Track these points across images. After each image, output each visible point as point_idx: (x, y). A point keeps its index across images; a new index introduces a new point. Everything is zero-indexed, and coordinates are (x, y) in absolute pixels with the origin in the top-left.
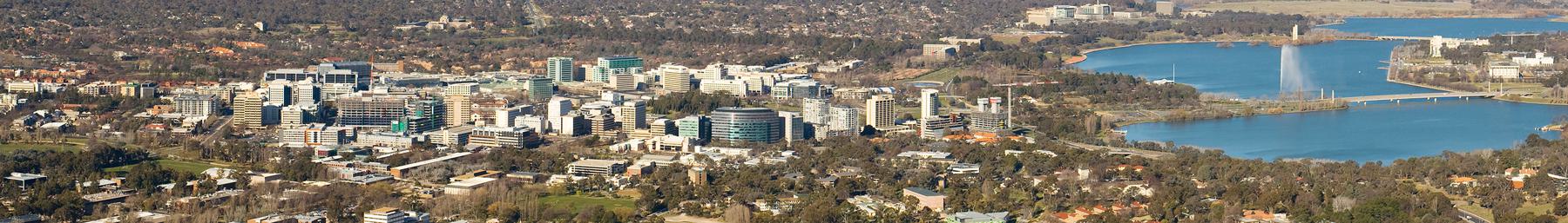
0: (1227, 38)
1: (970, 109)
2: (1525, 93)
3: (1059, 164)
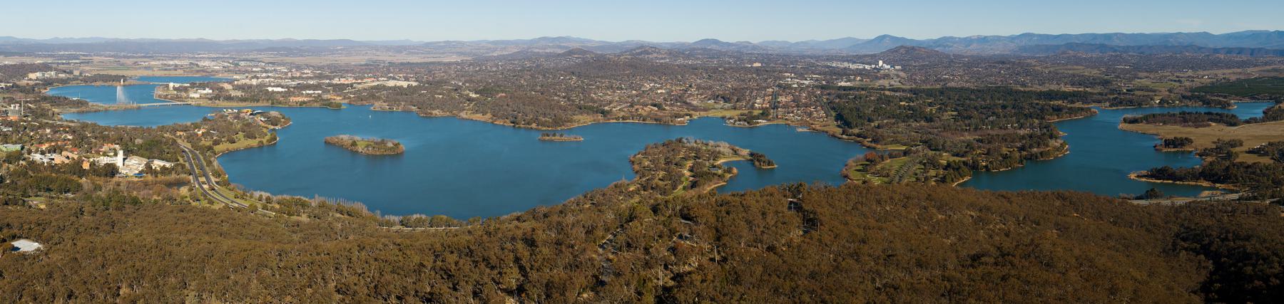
0: (98, 83)
1: (8, 108)
2: (203, 103)
3: (39, 128)
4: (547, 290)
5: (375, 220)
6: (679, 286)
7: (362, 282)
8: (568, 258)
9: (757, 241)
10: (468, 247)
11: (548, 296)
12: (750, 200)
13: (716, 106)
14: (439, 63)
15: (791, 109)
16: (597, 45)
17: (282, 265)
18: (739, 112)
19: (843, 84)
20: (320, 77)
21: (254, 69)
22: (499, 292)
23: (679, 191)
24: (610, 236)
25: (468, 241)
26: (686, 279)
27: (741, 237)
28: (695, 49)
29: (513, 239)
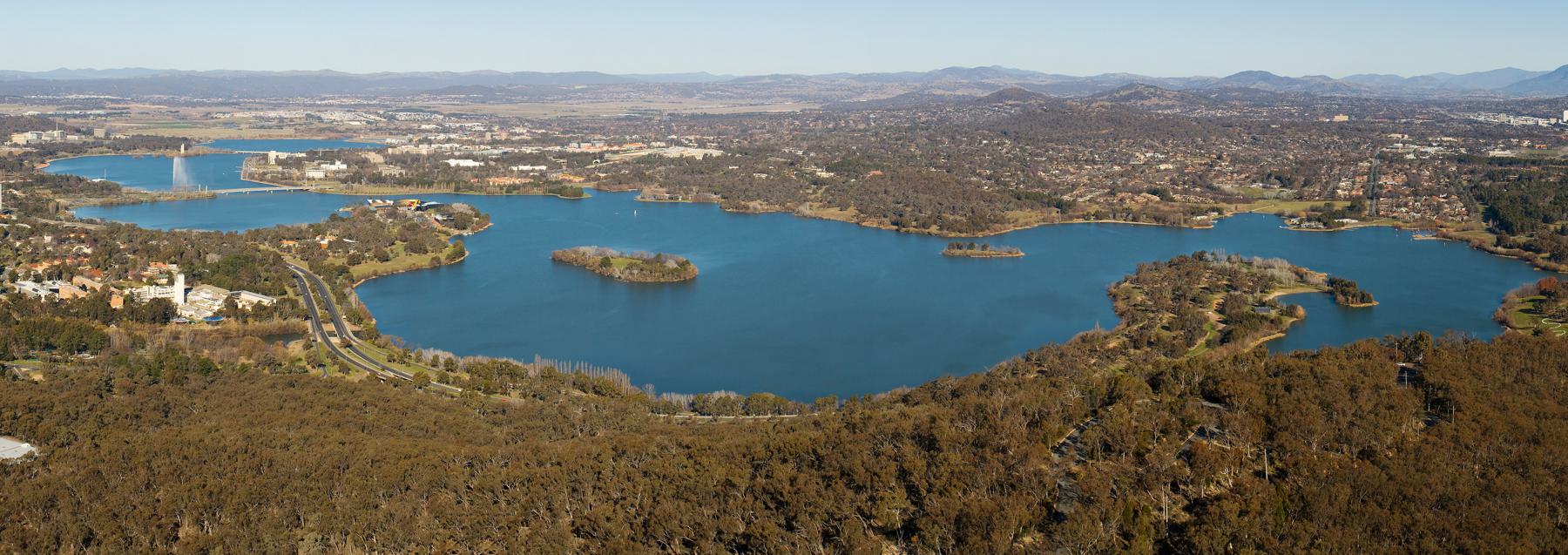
0: (139, 152)
2: (328, 187)
3: (32, 233)
4: (958, 529)
5: (645, 402)
6: (1199, 523)
7: (621, 515)
8: (996, 470)
9: (1341, 439)
10: (814, 451)
11: (960, 541)
12: (1329, 366)
13: (1267, 193)
14: (762, 116)
15: (1402, 200)
16: (1049, 81)
17: (474, 483)
18: (1307, 205)
19: (1498, 153)
20: (545, 140)
21: (424, 127)
22: (871, 533)
23: (1199, 348)
24: (1073, 432)
25: (815, 441)
26: (1212, 509)
27: (1311, 432)
28: (1226, 90)
29: (896, 436)
